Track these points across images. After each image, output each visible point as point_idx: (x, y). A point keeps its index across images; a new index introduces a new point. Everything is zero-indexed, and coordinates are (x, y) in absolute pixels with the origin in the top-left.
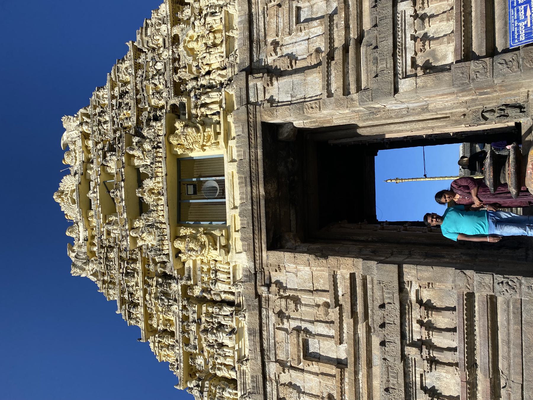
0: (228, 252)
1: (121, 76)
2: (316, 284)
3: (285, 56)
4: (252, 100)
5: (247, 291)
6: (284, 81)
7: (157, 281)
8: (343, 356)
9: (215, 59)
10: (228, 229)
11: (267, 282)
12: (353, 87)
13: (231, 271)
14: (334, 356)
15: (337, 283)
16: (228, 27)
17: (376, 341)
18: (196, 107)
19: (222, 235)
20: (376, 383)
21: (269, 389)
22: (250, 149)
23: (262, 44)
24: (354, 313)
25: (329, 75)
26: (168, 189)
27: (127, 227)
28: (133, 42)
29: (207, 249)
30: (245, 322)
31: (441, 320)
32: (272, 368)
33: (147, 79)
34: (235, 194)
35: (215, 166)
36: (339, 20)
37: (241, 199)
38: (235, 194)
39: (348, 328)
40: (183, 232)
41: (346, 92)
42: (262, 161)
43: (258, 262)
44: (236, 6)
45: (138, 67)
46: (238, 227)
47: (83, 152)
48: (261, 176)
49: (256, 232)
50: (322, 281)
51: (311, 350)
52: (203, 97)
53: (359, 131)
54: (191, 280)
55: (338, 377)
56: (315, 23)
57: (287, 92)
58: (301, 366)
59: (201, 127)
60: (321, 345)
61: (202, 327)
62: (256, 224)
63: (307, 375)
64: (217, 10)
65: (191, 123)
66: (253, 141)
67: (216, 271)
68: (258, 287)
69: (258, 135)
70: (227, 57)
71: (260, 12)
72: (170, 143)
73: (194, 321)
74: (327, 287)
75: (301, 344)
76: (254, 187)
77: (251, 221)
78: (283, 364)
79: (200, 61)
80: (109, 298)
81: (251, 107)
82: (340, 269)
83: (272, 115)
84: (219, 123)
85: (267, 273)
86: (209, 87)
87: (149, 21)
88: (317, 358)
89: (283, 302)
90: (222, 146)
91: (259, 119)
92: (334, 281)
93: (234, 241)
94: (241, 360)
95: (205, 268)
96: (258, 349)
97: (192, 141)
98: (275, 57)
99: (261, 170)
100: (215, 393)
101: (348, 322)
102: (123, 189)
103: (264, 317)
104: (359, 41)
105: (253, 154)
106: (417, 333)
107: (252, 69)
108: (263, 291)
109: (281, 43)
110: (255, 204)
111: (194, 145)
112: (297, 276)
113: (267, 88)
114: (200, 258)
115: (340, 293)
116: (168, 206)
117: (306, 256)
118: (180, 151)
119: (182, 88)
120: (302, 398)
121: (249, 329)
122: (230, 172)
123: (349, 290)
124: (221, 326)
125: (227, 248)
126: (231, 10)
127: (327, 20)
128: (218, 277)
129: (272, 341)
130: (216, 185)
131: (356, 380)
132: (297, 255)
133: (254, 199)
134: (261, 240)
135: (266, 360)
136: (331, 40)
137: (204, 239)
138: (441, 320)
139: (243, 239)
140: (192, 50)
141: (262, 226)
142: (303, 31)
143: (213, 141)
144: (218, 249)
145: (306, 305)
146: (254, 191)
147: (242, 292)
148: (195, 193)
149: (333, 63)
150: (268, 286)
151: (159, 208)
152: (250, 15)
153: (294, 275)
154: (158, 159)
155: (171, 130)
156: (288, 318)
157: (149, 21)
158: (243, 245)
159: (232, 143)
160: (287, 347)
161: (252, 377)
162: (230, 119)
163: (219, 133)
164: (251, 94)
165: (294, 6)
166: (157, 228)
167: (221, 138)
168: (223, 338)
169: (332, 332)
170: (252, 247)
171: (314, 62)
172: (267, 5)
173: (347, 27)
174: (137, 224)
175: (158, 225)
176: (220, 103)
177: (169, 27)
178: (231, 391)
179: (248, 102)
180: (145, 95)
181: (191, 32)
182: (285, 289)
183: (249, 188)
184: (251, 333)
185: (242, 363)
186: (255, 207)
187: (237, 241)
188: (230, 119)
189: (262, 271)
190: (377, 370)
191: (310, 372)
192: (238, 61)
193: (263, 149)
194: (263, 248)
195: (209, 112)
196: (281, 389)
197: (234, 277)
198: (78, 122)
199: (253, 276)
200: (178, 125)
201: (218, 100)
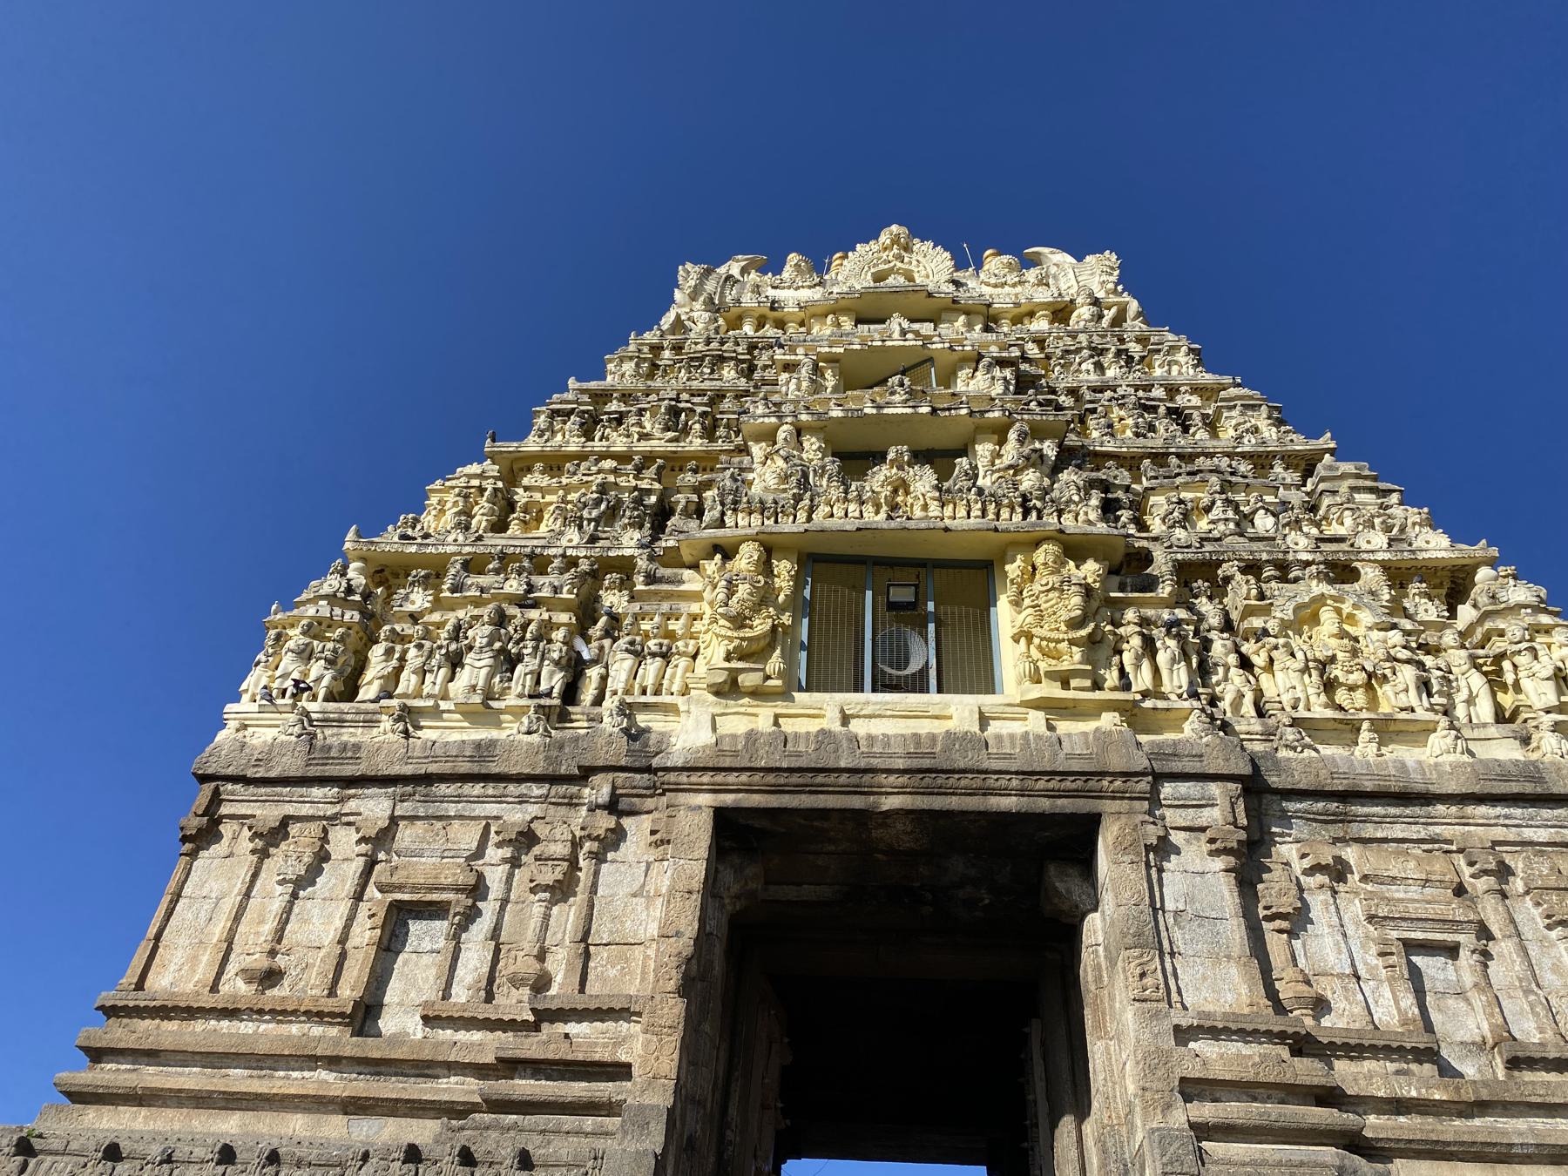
0: (717, 694)
1: (1234, 413)
2: (604, 953)
3: (1302, 899)
4: (1167, 789)
5: (601, 741)
6: (1223, 892)
7: (649, 492)
8: (388, 1024)
9: (1285, 684)
10: (784, 695)
11: (624, 804)
12: (1206, 1111)
13: (665, 698)
14: (391, 996)
15: (603, 1021)
16: (1386, 730)
17: (423, 1131)
18: (1144, 622)
19: (768, 678)
20: (297, 1125)
21: (317, 792)
22: (1017, 773)
23: (1337, 830)
24: (510, 1066)
25: (1245, 1035)
26: (904, 533)
27: (804, 417)
28: (1332, 452)
29: (730, 633)
30: (516, 734)
32: (374, 807)
33: (1227, 486)
34: (886, 723)
35: (970, 668)
36: (1418, 1083)
37: (871, 739)
38: (886, 723)
39: (469, 1046)
40: (784, 569)
41: (1192, 1089)
42: (982, 808)
43: (683, 778)
44: (1451, 758)
45: (1261, 461)
46: (788, 726)
47: (1018, 305)
48: (938, 803)
49: (771, 778)
50: (612, 972)
51: (415, 927)
52: (1172, 643)
53: (1067, 1123)
54: (647, 584)
55: (329, 1005)
56: (1408, 1001)
57: (1189, 898)
58: (372, 891)
59: (1083, 633)
60: (426, 959)
61: (513, 610)
62: (795, 779)
63: (344, 908)
64: (1436, 699)
65: (1097, 606)
66: (1041, 784)
67: (666, 656)
68: (611, 776)
69: (1060, 802)
70: (1295, 723)
71: (1438, 829)
72: (1037, 544)
73: (531, 588)
74: (593, 987)
75: (435, 897)
76: (904, 779)
77: (804, 765)
78: (383, 838)
79: (1281, 641)
80: (611, 361)
81: (1144, 785)
82: (646, 1032)
83: (1121, 847)
84: (1097, 685)
85: (650, 803)
86: (1202, 663)
87: (1394, 498)
88: (390, 944)
89: (561, 849)
90: (1028, 691)
91: (1107, 806)
92: (611, 1010)
93: (750, 710)
94: (409, 717)
95: (676, 626)
96: (433, 768)
97: (1044, 606)
98: (1298, 866)
99: (954, 803)
100: (322, 639)
101: (484, 1045)
102: (909, 411)
103: (523, 788)
104: (1355, 1143)
105: (1003, 783)
108: (598, 789)
109: (1341, 887)
110: (855, 779)
111: (1030, 611)
112: (634, 895)
113: (1204, 837)
114: (707, 612)
115: (573, 1028)
116: (859, 529)
117: (690, 928)
118: (1013, 569)
119: (1200, 584)
120: (280, 889)
121: (492, 743)
122: (952, 711)
123: (580, 1057)
124: (508, 662)
125: (728, 689)
126: (1440, 740)
127: (1421, 1041)
128: (649, 661)
129: (452, 810)
130: (914, 666)
131: (312, 1061)
132: (696, 899)
133: (867, 778)
134: (747, 791)
135: (399, 790)
136: (1355, 1050)
137: (760, 626)
139: (752, 736)
140: (1315, 620)
141: (787, 797)
142: (1380, 962)
143: (1043, 666)
144: (727, 665)
145: (547, 917)
146: (892, 778)
148: (892, 606)
149: (1284, 1052)
150: (612, 807)
151: (852, 507)
152: (1427, 798)
153: (636, 886)
154: (991, 508)
155: (1074, 549)
156: (515, 863)
157: (1394, 498)
158: (734, 737)
159: (1036, 722)
160: (430, 855)
161: (357, 747)
162: (1109, 720)
163: (1066, 685)
164: (1184, 788)
165: (1460, 938)
166: (798, 499)
167: (1054, 690)
168: (476, 669)
169: (460, 994)
170: (727, 763)
171: (1285, 991)
172: (1461, 851)
173: (1398, 1106)
174: (811, 444)
175: (807, 502)
176: (1155, 692)
177: (1380, 556)
178: (325, 682)
179: (1159, 778)
180: (1178, 480)
181: (1366, 618)
182: (599, 858)
183: (900, 764)
184: (483, 750)
185: (399, 719)
186: (844, 778)
188: (1109, 721)
189: (655, 790)
190: (336, 1129)
191: (351, 919)
192: (1283, 753)
193: (1018, 813)
194: (722, 797)
195: (1128, 658)
196: (314, 828)
197: (646, 707)
198: (1100, 295)
199: (643, 763)
200: (1091, 569)
201: (1166, 688)
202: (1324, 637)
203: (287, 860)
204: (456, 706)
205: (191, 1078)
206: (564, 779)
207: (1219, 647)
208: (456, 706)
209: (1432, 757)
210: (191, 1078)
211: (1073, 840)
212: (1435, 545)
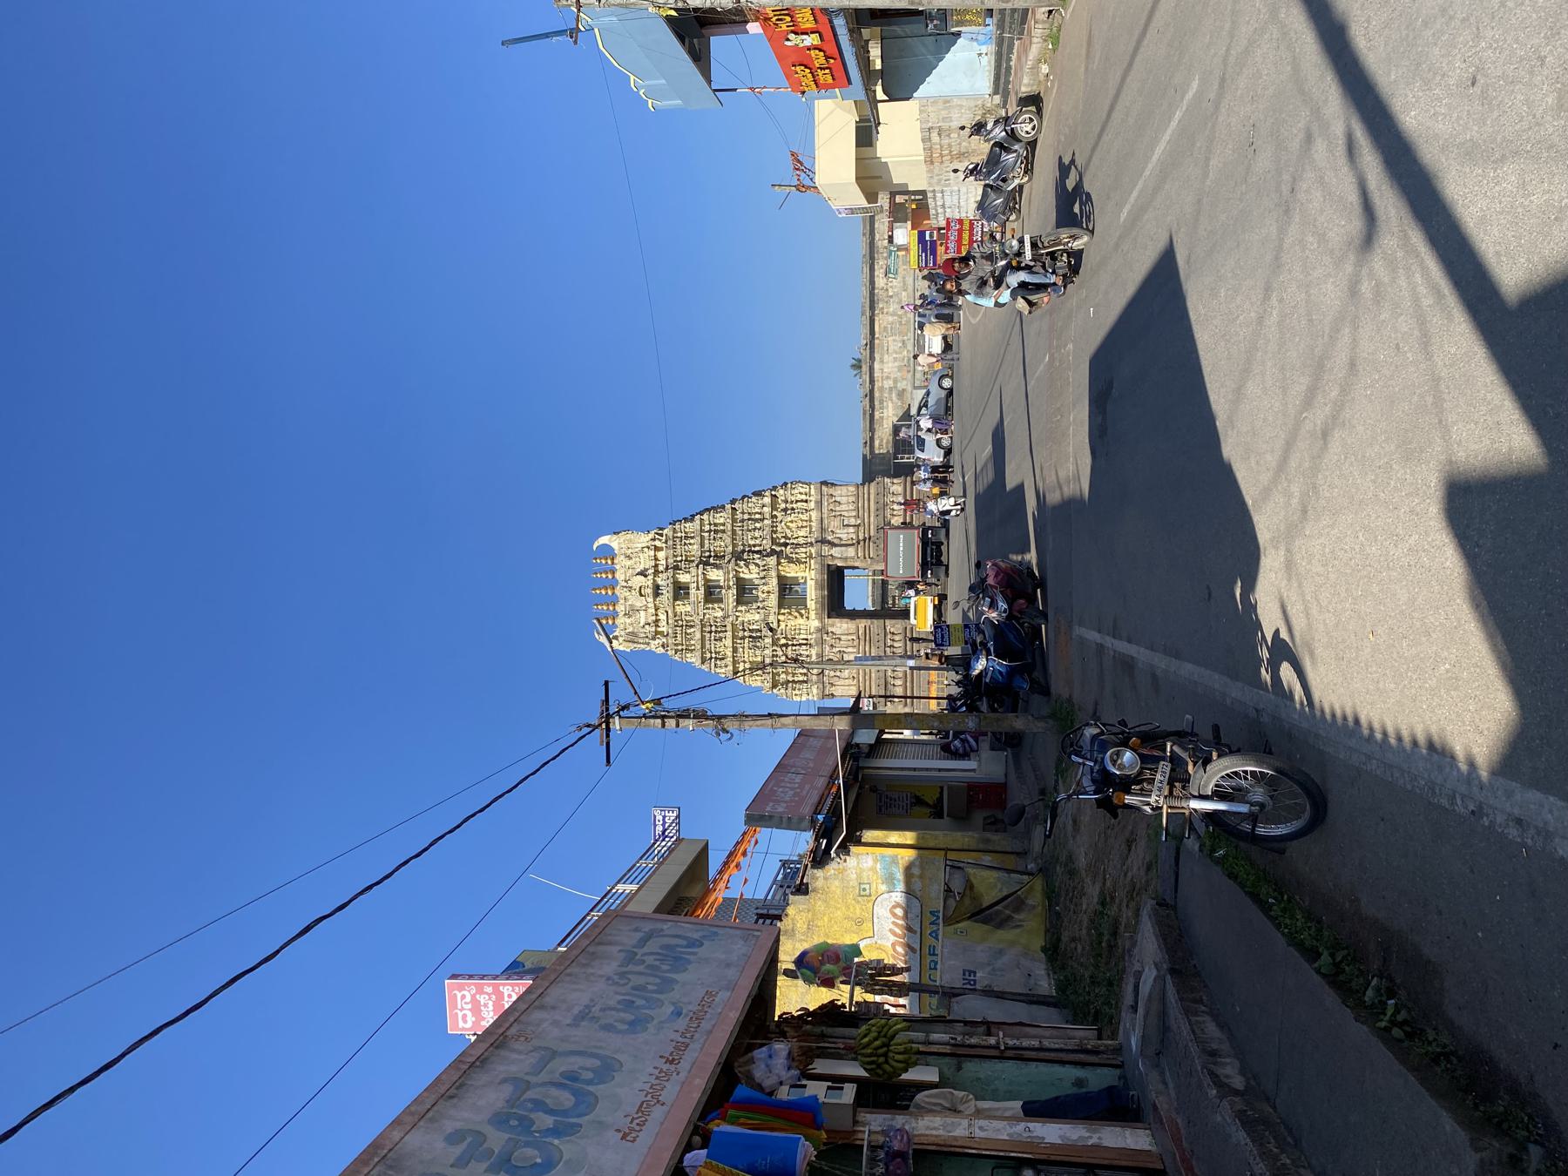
9: (802, 533)
45: (734, 520)
65: (790, 560)
106: (889, 643)
107: (823, 541)
147: (813, 638)
155: (779, 564)
187: (813, 615)
202: (793, 525)
206: (823, 642)
209: (814, 515)
212: (767, 500)
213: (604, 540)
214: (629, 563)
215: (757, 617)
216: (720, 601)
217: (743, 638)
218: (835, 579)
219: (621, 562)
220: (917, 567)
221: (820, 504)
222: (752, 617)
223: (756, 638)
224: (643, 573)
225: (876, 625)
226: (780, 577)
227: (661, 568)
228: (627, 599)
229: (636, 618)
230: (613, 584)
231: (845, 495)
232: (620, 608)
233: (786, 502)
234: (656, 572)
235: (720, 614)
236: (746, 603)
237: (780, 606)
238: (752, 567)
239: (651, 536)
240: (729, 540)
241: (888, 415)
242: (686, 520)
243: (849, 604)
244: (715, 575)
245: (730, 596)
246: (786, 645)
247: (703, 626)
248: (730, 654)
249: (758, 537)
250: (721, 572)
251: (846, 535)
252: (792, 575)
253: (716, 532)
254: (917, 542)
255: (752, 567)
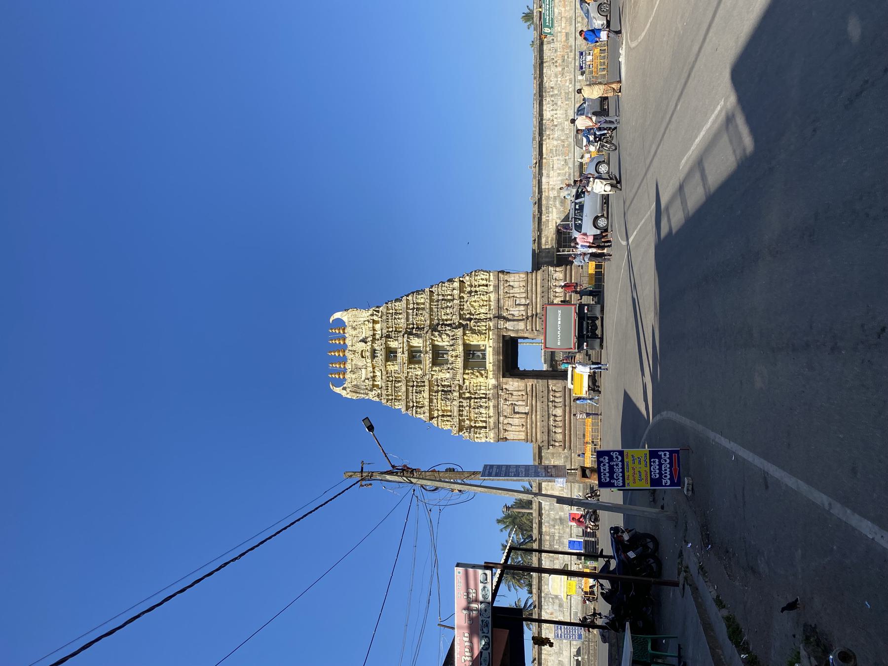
6: (511, 323)
16: (490, 301)
30: (491, 404)
31: (557, 395)
32: (501, 419)
36: (530, 307)
45: (431, 300)
65: (473, 332)
88: (518, 413)
94: (490, 417)
101: (530, 398)
107: (499, 317)
124: (481, 406)
125: (487, 377)
138: (557, 395)
155: (464, 334)
159: (491, 341)
160: (507, 410)
184: (494, 407)
187: (491, 375)
203: (509, 428)
204: (488, 412)
205: (534, 430)
207: (478, 317)
208: (488, 412)
209: (493, 296)
210: (534, 430)
211: (504, 336)
213: (337, 315)
214: (354, 333)
215: (448, 375)
216: (420, 362)
217: (437, 392)
218: (509, 348)
219: (349, 330)
220: (573, 340)
221: (497, 288)
222: (443, 375)
223: (446, 392)
224: (364, 341)
225: (540, 384)
226: (465, 345)
227: (377, 337)
228: (353, 360)
229: (359, 375)
230: (344, 348)
231: (517, 281)
232: (348, 366)
233: (471, 286)
234: (374, 340)
235: (420, 373)
236: (439, 365)
237: (465, 367)
238: (444, 337)
239: (370, 312)
240: (427, 316)
241: (553, 218)
242: (396, 300)
243: (524, 364)
244: (416, 342)
245: (427, 359)
246: (470, 398)
247: (407, 381)
248: (426, 403)
249: (450, 314)
250: (421, 340)
251: (518, 312)
252: (475, 343)
253: (418, 309)
254: (574, 317)
255: (444, 337)
